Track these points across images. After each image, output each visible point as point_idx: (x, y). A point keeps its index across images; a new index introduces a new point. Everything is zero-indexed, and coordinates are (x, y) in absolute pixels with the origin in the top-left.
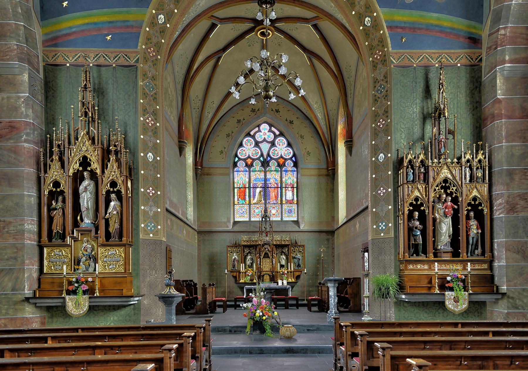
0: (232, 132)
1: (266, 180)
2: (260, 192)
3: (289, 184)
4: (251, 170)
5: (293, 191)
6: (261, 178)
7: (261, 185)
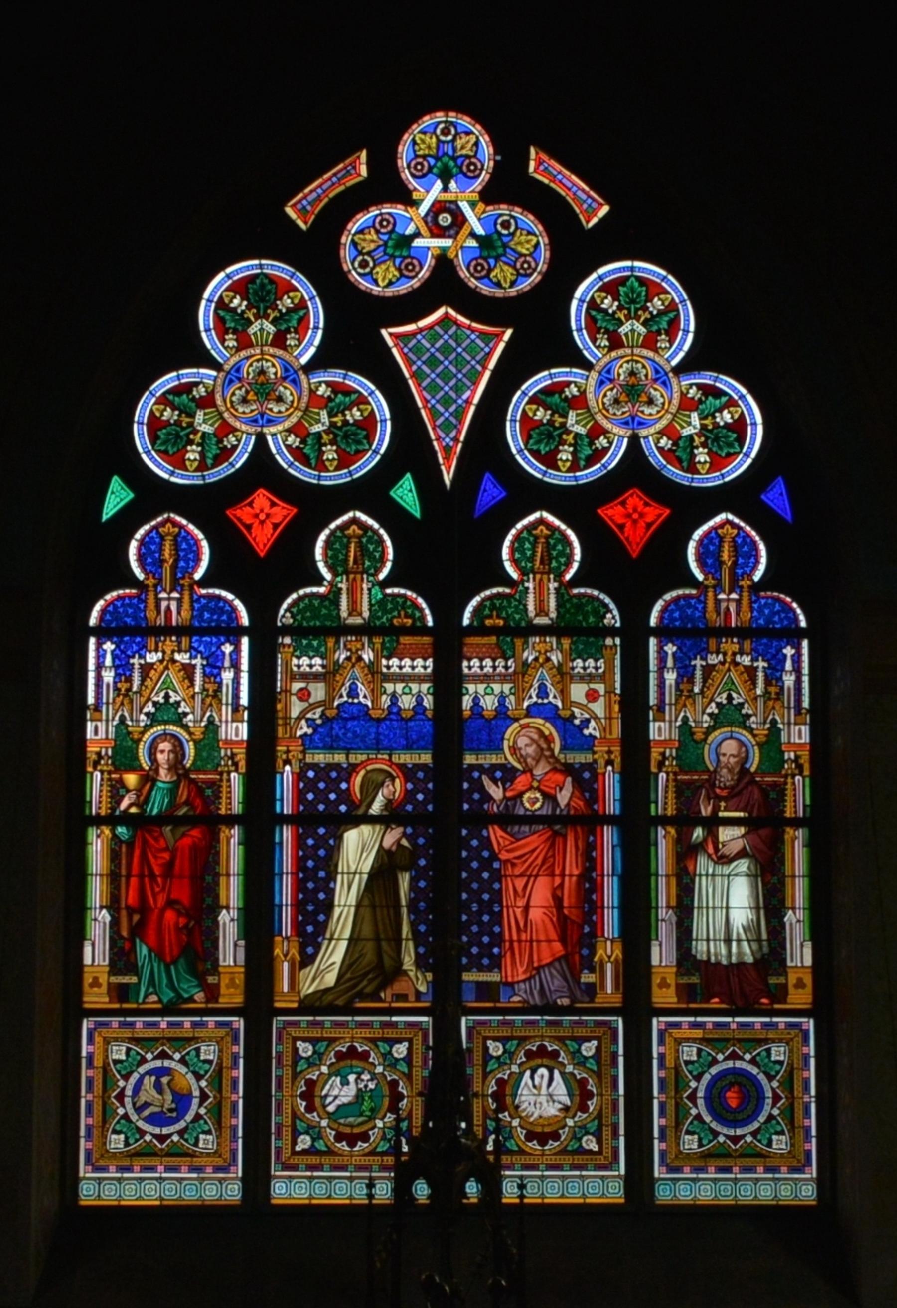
3: (726, 777)
4: (284, 614)
7: (395, 788)
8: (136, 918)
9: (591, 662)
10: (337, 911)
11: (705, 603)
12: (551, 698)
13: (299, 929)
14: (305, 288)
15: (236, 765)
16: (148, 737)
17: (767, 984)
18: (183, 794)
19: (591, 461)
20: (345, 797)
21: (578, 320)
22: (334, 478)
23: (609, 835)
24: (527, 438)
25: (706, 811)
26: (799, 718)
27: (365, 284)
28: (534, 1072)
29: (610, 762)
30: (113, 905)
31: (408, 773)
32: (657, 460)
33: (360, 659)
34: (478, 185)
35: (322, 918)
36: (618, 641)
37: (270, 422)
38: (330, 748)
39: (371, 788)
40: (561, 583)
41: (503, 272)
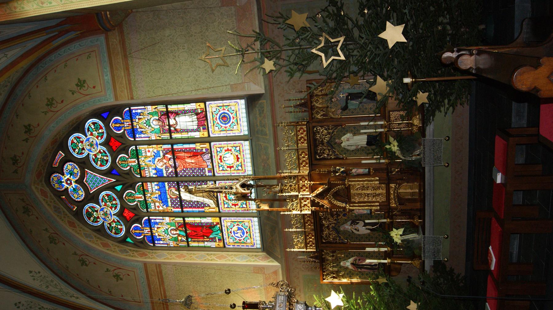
0: (75, 254)
1: (160, 178)
2: (190, 192)
5: (177, 114)
6: (159, 190)
7: (173, 190)
8: (205, 237)
9: (143, 152)
10: (198, 200)
11: (127, 129)
12: (151, 159)
13: (203, 208)
14: (86, 207)
15: (174, 219)
16: (172, 235)
17: (201, 113)
18: (181, 229)
19: (106, 153)
20: (176, 199)
21: (81, 156)
23: (175, 147)
24: (104, 166)
25: (167, 127)
26: (146, 108)
27: (83, 196)
28: (224, 161)
29: (161, 147)
30: (204, 242)
31: (170, 187)
33: (150, 196)
34: (61, 176)
35: (200, 203)
36: (138, 146)
37: (111, 213)
40: (129, 158)
41: (75, 171)
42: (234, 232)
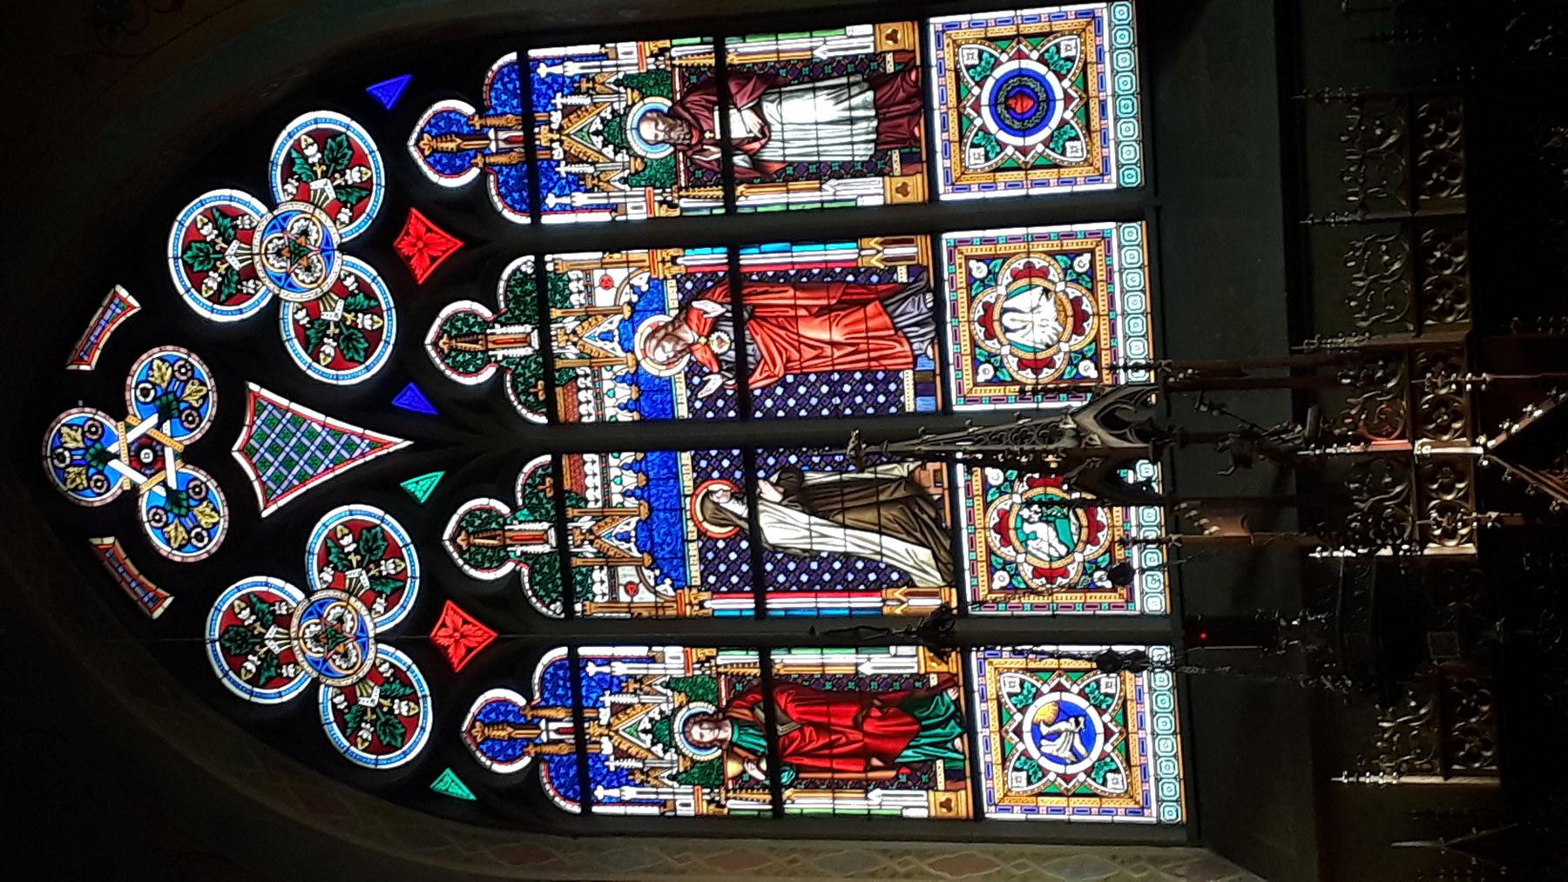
6: (639, 493)
7: (720, 491)
8: (876, 762)
9: (573, 286)
10: (851, 549)
11: (501, 165)
12: (613, 327)
13: (872, 589)
14: (230, 597)
15: (708, 659)
16: (689, 750)
17: (896, 74)
19: (371, 295)
20: (731, 543)
21: (232, 313)
22: (412, 562)
23: (750, 258)
24: (353, 362)
25: (715, 154)
26: (611, 55)
27: (219, 536)
28: (1007, 330)
29: (673, 260)
30: (864, 786)
31: (702, 477)
32: (362, 224)
33: (590, 531)
34: (110, 423)
35: (860, 565)
36: (548, 258)
37: (363, 629)
38: (683, 559)
39: (720, 516)
40: (495, 321)
41: (192, 393)
42: (1035, 727)
